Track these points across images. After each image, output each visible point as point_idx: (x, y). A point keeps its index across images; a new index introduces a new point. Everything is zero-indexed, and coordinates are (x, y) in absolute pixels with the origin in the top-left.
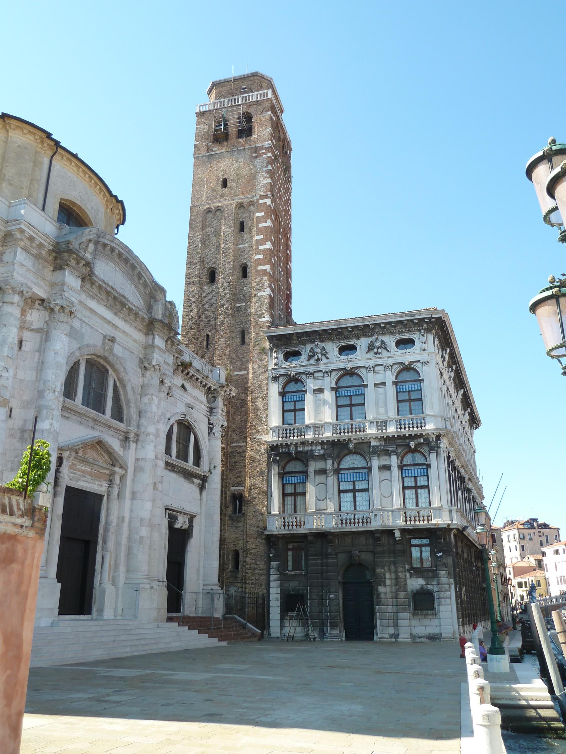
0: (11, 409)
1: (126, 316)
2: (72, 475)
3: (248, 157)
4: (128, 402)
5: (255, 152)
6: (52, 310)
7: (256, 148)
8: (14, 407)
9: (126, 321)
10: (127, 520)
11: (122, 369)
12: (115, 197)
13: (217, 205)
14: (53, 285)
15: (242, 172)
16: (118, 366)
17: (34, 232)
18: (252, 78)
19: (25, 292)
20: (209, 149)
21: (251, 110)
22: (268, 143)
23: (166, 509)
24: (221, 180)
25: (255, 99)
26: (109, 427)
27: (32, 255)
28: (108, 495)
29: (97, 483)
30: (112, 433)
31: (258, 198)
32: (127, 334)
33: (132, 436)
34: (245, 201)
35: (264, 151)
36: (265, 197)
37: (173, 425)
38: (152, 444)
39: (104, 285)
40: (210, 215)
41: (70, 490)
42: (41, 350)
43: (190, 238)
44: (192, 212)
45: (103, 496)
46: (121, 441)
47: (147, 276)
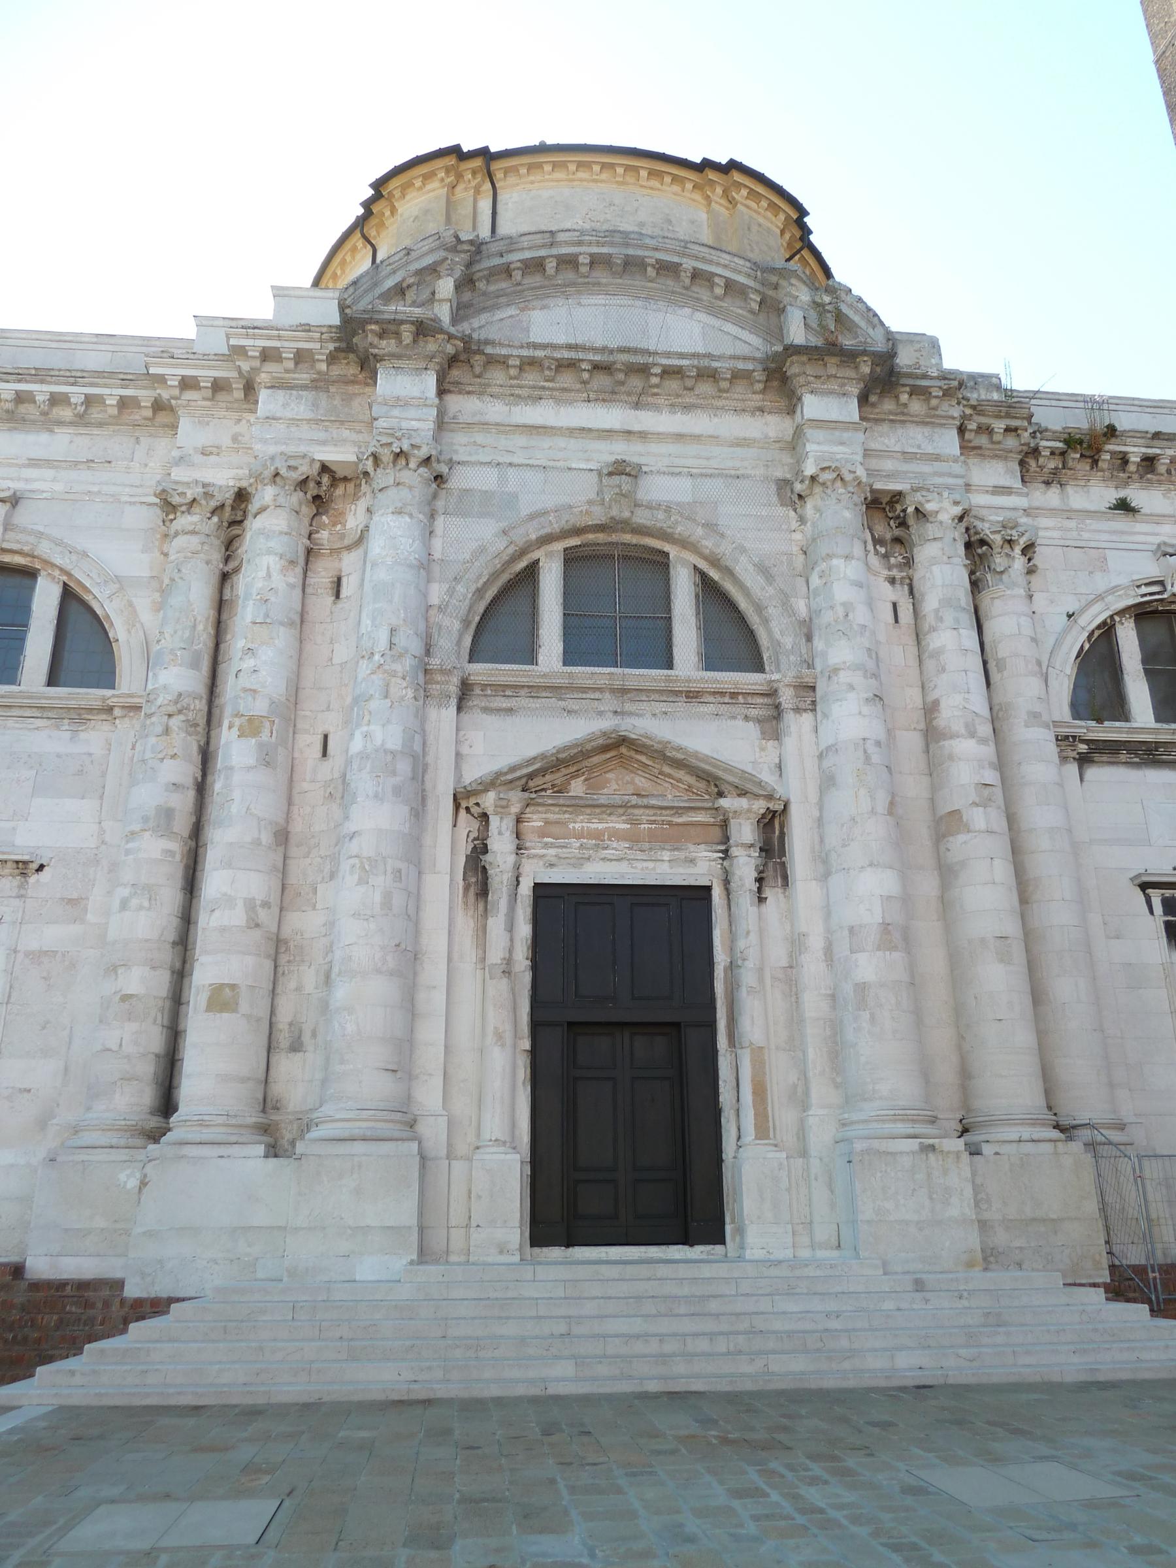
0: (326, 737)
1: (678, 396)
2: (552, 851)
4: (759, 609)
8: (331, 730)
9: (687, 408)
10: (816, 943)
11: (700, 531)
12: (707, 165)
16: (679, 529)
17: (269, 338)
19: (283, 472)
23: (1144, 886)
26: (693, 696)
27: (304, 387)
28: (726, 882)
29: (666, 855)
30: (711, 708)
32: (697, 438)
33: (787, 697)
37: (1106, 632)
38: (852, 696)
39: (540, 353)
45: (708, 889)
46: (759, 721)
47: (725, 266)
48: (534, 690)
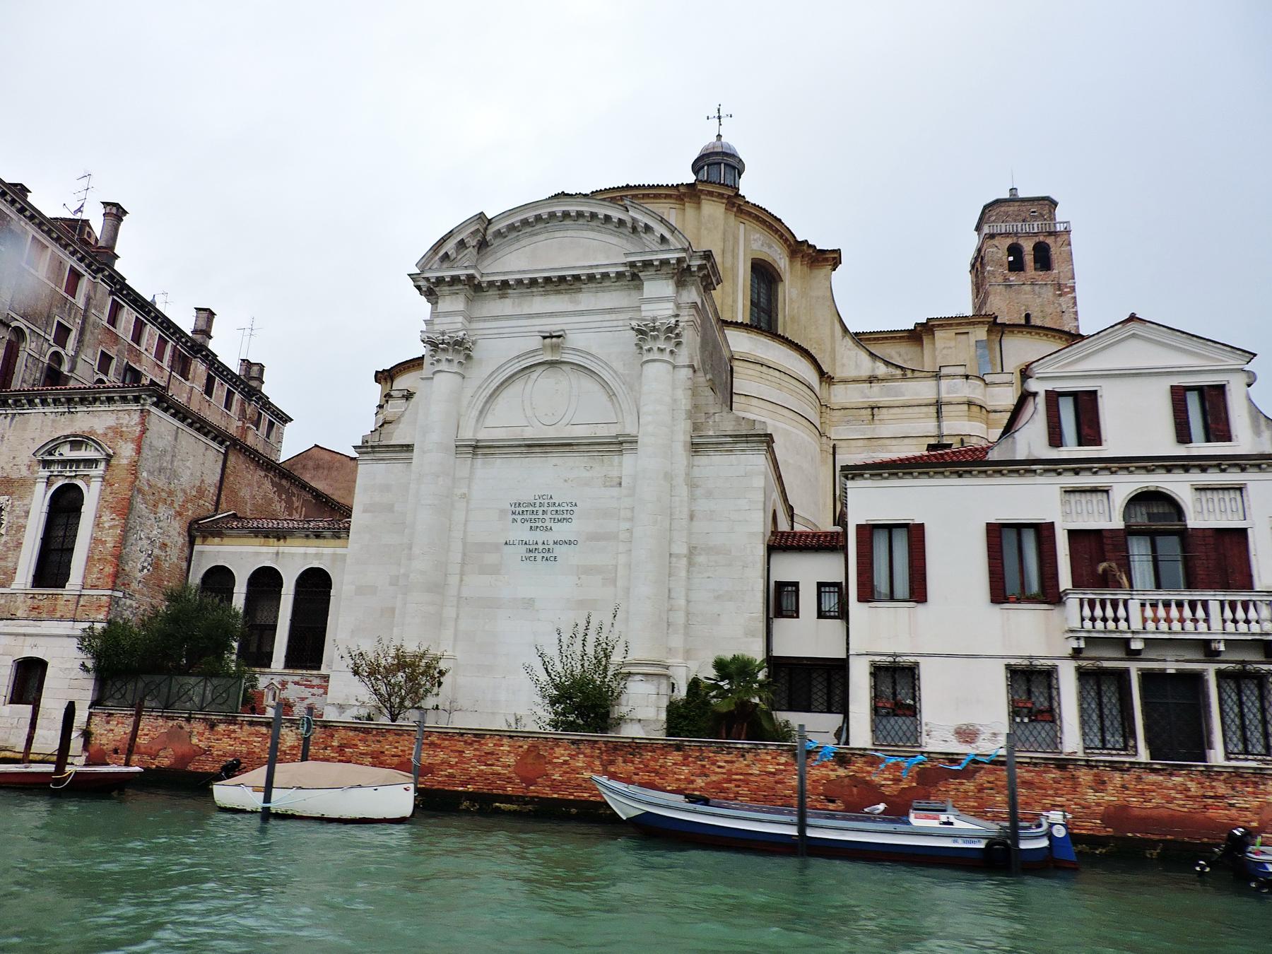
3: (1050, 294)
5: (1059, 290)
7: (1059, 285)
15: (1046, 309)
18: (1041, 202)
20: (1006, 279)
21: (1050, 241)
24: (1024, 315)
35: (1068, 290)
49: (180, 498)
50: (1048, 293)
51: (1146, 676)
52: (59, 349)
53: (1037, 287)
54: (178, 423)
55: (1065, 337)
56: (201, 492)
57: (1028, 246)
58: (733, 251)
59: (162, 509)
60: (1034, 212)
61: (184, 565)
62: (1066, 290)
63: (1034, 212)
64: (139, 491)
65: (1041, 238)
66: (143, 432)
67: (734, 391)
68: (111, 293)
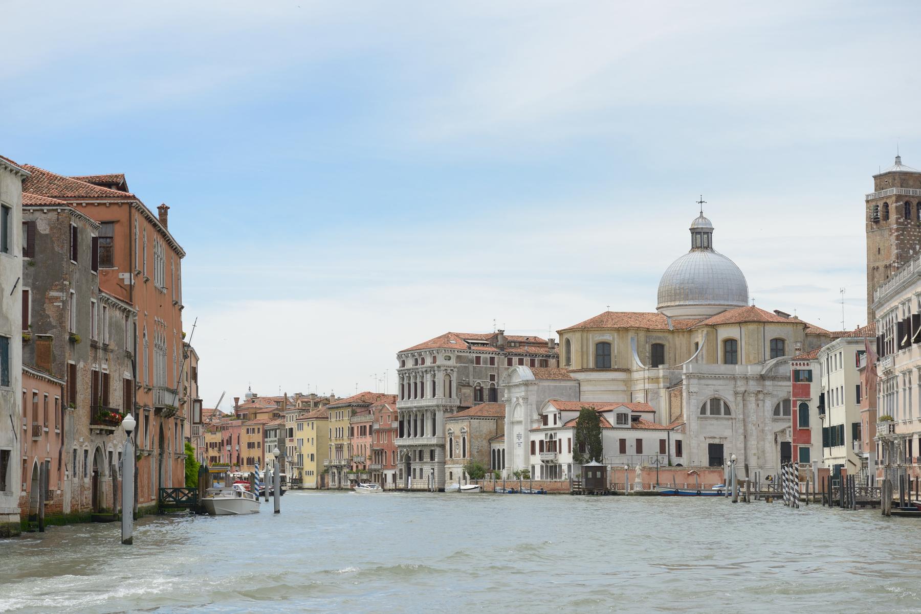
5: (891, 231)
6: (764, 394)
13: (877, 265)
14: (763, 385)
18: (889, 175)
20: (872, 228)
22: (895, 226)
25: (889, 194)
31: (892, 262)
34: (888, 264)
36: (894, 262)
40: (875, 271)
41: (782, 443)
42: (764, 406)
43: (868, 286)
44: (868, 269)
48: (780, 419)
49: (484, 435)
50: (886, 233)
51: (550, 466)
52: (493, 382)
53: (883, 231)
54: (479, 420)
55: (737, 325)
56: (491, 432)
57: (881, 204)
58: (587, 343)
59: (479, 439)
60: (886, 182)
61: (489, 449)
62: (893, 231)
63: (886, 182)
64: (472, 437)
65: (885, 201)
66: (470, 425)
67: (581, 390)
68: (506, 357)
